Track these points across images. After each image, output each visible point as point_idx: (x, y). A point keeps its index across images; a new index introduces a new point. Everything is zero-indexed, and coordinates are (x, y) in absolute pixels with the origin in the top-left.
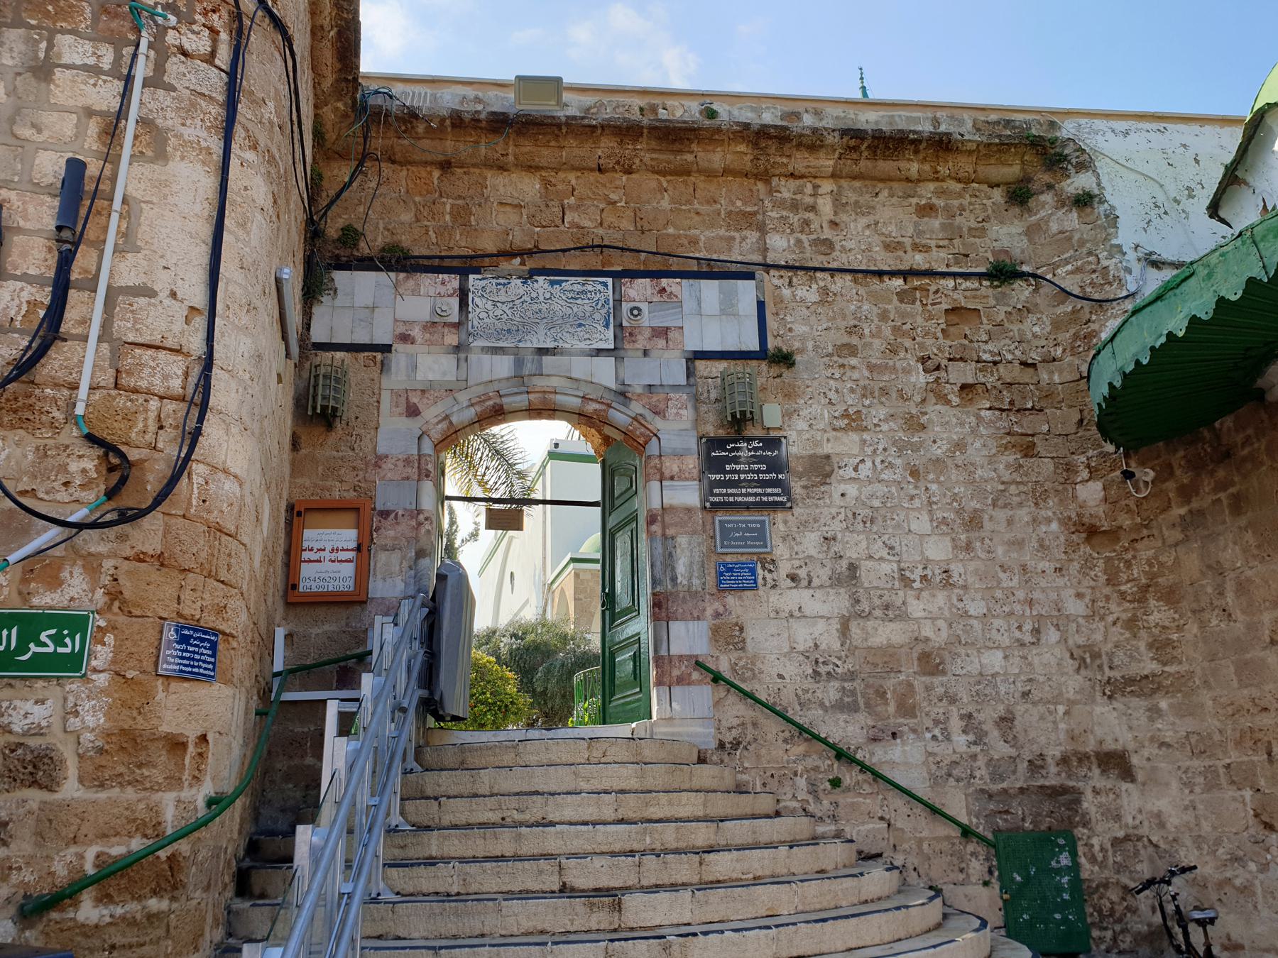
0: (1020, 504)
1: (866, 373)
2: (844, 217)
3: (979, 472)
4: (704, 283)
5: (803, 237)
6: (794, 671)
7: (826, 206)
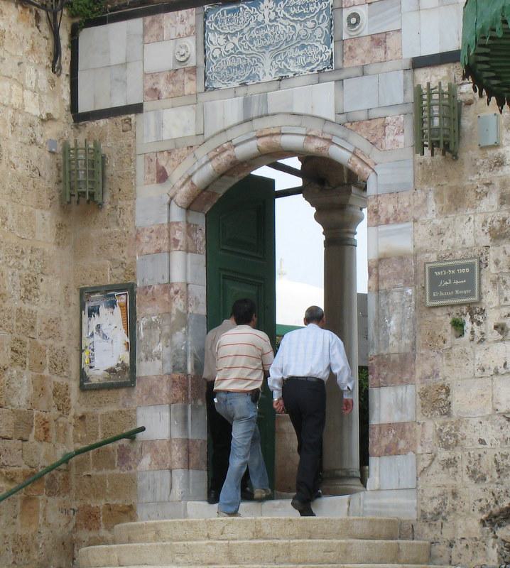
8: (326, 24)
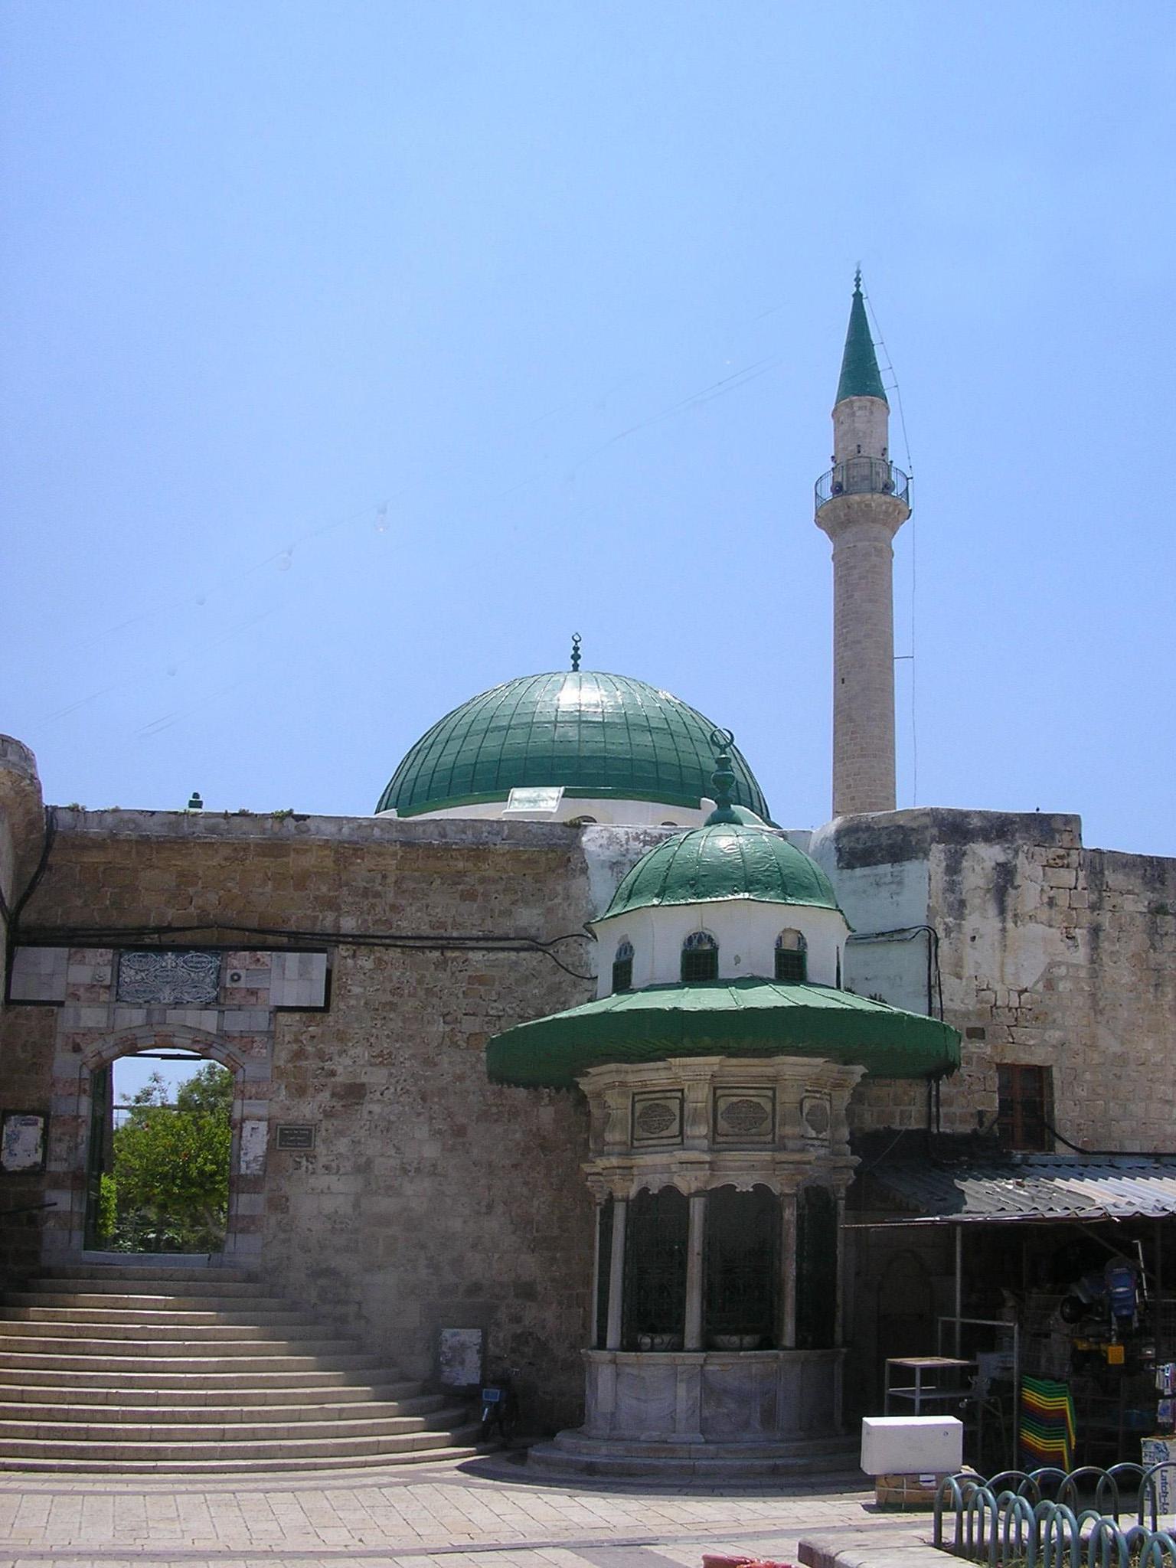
4: (288, 954)
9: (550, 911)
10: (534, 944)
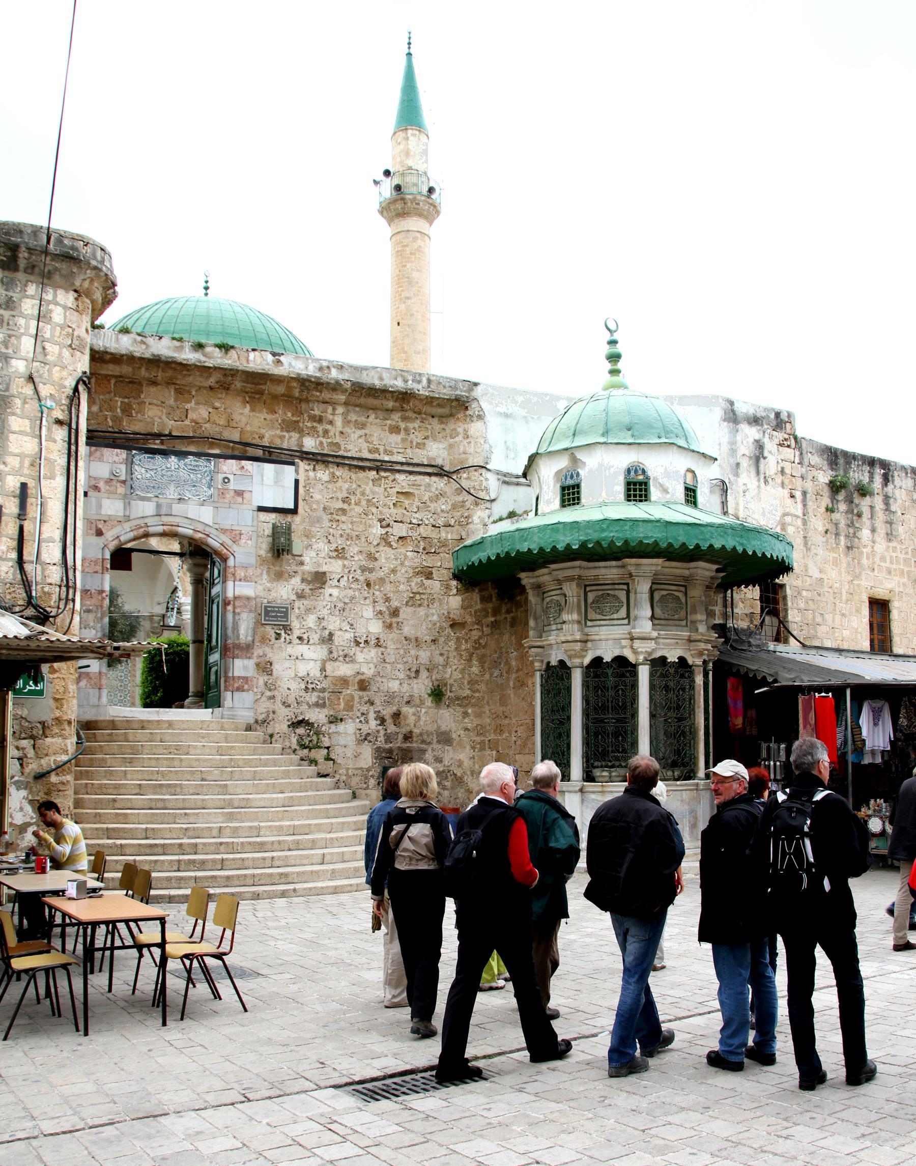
0: (420, 605)
1: (350, 526)
2: (347, 430)
3: (402, 586)
5: (324, 440)
6: (296, 687)
7: (339, 421)
8: (208, 478)
9: (451, 446)
10: (441, 472)
